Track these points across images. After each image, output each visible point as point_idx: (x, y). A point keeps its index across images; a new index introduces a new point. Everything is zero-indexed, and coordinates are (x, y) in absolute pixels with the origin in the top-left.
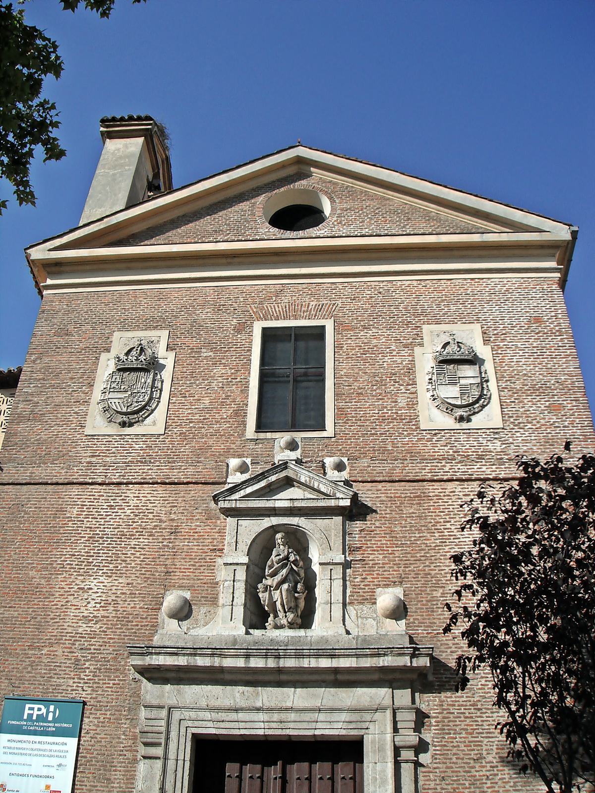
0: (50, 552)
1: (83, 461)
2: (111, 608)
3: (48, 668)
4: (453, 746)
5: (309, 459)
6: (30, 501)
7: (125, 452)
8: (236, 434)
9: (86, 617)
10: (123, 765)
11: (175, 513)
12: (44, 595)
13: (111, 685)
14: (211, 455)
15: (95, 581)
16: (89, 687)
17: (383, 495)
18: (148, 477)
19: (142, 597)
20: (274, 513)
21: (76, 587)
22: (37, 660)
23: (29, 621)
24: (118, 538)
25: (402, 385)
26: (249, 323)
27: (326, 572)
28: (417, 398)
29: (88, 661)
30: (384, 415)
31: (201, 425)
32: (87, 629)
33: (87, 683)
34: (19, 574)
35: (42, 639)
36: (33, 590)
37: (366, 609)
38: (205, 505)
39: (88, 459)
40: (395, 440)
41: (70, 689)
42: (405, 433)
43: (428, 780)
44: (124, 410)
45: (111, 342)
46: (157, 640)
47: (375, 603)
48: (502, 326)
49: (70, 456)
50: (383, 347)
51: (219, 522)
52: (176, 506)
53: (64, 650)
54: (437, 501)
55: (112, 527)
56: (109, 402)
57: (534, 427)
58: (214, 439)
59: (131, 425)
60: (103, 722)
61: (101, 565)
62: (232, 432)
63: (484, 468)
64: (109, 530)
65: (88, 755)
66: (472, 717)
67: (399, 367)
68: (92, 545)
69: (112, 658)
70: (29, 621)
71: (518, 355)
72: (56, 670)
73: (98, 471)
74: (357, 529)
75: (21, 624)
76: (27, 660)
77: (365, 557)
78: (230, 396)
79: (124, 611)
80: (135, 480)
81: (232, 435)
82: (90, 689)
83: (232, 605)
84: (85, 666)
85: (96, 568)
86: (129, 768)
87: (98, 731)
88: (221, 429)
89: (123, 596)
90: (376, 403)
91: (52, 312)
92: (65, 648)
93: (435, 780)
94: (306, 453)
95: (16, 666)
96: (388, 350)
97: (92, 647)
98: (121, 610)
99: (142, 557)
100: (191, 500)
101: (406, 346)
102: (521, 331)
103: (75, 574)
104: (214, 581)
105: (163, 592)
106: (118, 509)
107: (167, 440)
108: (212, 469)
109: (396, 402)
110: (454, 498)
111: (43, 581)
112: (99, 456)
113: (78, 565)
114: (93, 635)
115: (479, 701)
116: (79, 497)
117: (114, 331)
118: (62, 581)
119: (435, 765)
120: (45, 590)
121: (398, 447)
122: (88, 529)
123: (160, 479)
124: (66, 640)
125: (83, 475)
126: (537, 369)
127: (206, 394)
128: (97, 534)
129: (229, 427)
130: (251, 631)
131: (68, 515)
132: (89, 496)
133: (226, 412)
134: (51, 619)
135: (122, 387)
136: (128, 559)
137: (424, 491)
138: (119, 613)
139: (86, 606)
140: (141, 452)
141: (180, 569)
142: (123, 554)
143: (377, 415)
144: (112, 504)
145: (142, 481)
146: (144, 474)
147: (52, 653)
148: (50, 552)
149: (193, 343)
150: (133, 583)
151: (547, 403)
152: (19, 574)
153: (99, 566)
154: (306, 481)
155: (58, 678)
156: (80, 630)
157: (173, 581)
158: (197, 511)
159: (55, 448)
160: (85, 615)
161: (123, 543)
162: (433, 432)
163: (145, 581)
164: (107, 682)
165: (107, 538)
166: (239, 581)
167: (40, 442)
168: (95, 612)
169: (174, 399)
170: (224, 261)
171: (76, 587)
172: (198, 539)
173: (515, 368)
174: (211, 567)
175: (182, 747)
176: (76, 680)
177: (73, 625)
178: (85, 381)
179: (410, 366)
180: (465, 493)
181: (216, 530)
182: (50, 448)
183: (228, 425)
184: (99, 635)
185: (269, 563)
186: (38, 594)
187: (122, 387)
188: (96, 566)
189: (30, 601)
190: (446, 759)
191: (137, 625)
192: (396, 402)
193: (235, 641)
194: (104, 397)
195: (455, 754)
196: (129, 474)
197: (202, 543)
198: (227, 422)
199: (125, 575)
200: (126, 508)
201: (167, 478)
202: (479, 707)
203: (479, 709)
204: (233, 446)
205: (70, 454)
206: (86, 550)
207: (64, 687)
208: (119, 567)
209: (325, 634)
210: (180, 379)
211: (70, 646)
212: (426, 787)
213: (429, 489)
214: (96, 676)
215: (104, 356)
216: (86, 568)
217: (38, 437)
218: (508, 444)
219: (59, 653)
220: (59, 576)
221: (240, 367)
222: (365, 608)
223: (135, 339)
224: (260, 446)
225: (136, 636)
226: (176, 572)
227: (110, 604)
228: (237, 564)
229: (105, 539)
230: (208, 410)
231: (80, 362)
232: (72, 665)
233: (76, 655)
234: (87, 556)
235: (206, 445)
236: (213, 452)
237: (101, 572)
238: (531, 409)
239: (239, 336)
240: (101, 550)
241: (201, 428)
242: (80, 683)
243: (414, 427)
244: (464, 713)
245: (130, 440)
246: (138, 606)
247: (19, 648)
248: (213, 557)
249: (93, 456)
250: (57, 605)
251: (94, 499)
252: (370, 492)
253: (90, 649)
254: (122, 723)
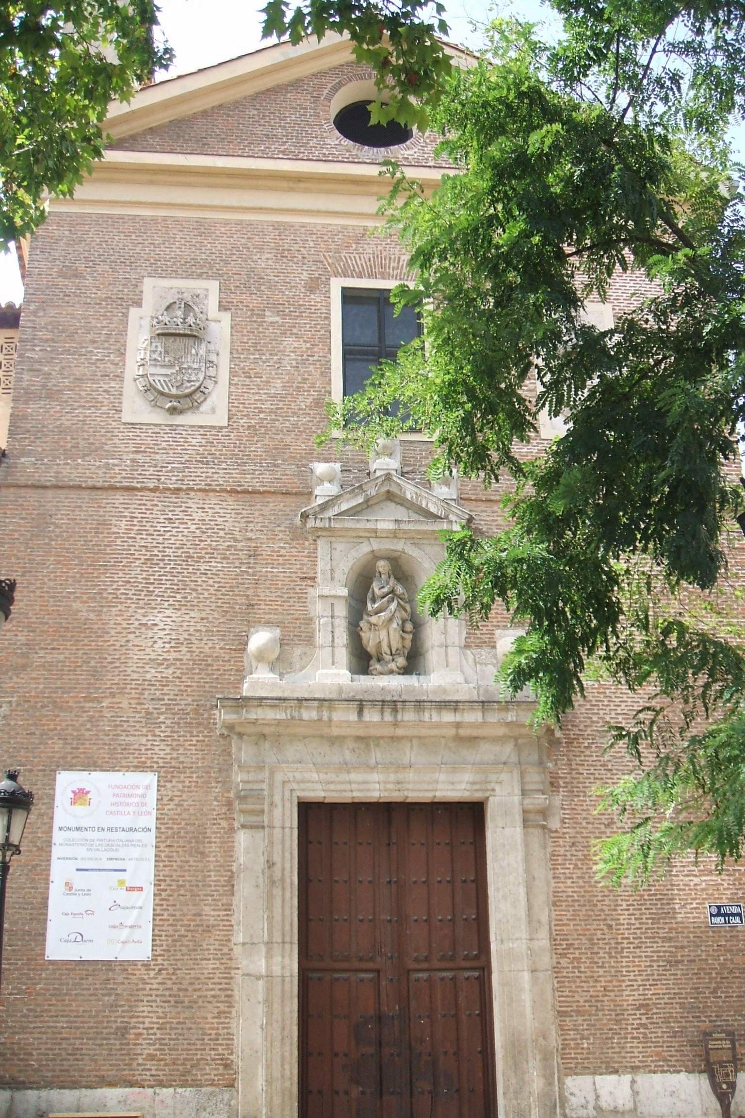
0: (97, 577)
1: (124, 457)
2: (184, 649)
3: (113, 724)
4: (583, 810)
5: (411, 468)
6: (59, 510)
7: (179, 448)
9: (154, 660)
10: (219, 835)
11: (252, 530)
12: (96, 632)
13: (194, 742)
14: (290, 457)
15: (160, 615)
16: (167, 745)
17: (499, 518)
18: (213, 483)
19: (222, 635)
20: (374, 535)
21: (137, 623)
22: (97, 715)
23: (80, 666)
24: (184, 561)
26: (323, 278)
29: (162, 713)
31: (274, 417)
32: (156, 675)
33: (164, 740)
34: (59, 606)
35: (100, 688)
36: (80, 627)
37: (484, 653)
38: (288, 522)
39: (131, 456)
41: (143, 748)
43: (557, 846)
44: (174, 391)
45: (142, 292)
46: (246, 690)
47: (494, 647)
49: (106, 451)
51: (307, 543)
52: (252, 522)
53: (131, 701)
55: (173, 546)
56: (151, 379)
59: (181, 412)
60: (189, 787)
61: (166, 595)
64: (171, 551)
65: (175, 826)
66: (602, 779)
68: (151, 570)
69: (192, 710)
70: (80, 666)
72: (122, 726)
73: (147, 473)
75: (70, 671)
76: (84, 715)
78: (306, 379)
79: (201, 652)
80: (198, 487)
82: (169, 748)
83: (333, 646)
84: (160, 720)
85: (159, 599)
86: (226, 840)
87: (184, 797)
88: (300, 423)
89: (198, 634)
91: (48, 240)
92: (133, 698)
93: (565, 846)
95: (70, 723)
97: (166, 697)
98: (198, 650)
99: (216, 585)
100: (270, 515)
103: (133, 606)
104: (308, 616)
105: (246, 629)
106: (180, 523)
107: (232, 435)
108: (294, 475)
111: (92, 616)
112: (146, 452)
113: (135, 594)
114: (165, 682)
115: (610, 761)
116: (126, 506)
117: (143, 277)
118: (116, 615)
119: (565, 830)
120: (96, 626)
122: (144, 549)
123: (229, 486)
124: (131, 689)
125: (128, 478)
127: (276, 374)
128: (156, 555)
129: (310, 421)
130: (356, 677)
131: (115, 530)
132: (140, 505)
133: (305, 401)
134: (109, 663)
135: (167, 359)
136: (199, 588)
138: (194, 654)
139: (152, 646)
140: (201, 449)
141: (265, 600)
142: (192, 581)
144: (170, 516)
145: (207, 488)
146: (208, 480)
147: (116, 706)
148: (97, 577)
149: (254, 302)
150: (207, 618)
152: (59, 606)
153: (163, 596)
154: (412, 497)
155: (127, 736)
156: (148, 676)
157: (258, 616)
158: (279, 528)
159: (84, 439)
160: (153, 657)
161: (191, 568)
163: (223, 616)
164: (189, 738)
165: (169, 560)
166: (338, 617)
167: (62, 431)
168: (165, 654)
169: (236, 379)
170: (285, 184)
171: (137, 623)
172: (284, 564)
174: (302, 597)
175: (288, 813)
176: (150, 738)
177: (138, 670)
178: (112, 347)
181: (305, 554)
182: (77, 439)
183: (308, 419)
184: (172, 682)
185: (370, 595)
186: (88, 631)
187: (167, 359)
188: (159, 596)
189: (78, 641)
190: (576, 823)
191: (219, 670)
193: (340, 689)
194: (143, 371)
195: (585, 819)
196: (189, 478)
197: (289, 568)
198: (306, 414)
199: (196, 608)
200: (190, 523)
201: (239, 486)
202: (610, 767)
203: (610, 770)
205: (106, 447)
206: (144, 576)
207: (136, 747)
208: (189, 598)
210: (240, 351)
211: (137, 696)
212: (556, 853)
214: (174, 732)
215: (134, 312)
216: (146, 598)
217: (58, 423)
219: (125, 704)
220: (113, 609)
221: (317, 340)
222: (483, 653)
223: (174, 291)
225: (218, 683)
226: (260, 605)
227: (182, 644)
228: (335, 597)
229: (166, 562)
230: (283, 398)
231: (102, 318)
232: (142, 720)
233: (146, 707)
234: (146, 583)
237: (166, 603)
239: (312, 296)
240: (163, 575)
241: (274, 420)
242: (155, 741)
244: (594, 774)
245: (184, 433)
246: (218, 647)
247: (71, 700)
248: (303, 587)
249: (137, 452)
250: (114, 645)
251: (147, 509)
252: (485, 514)
253: (164, 700)
254: (212, 787)
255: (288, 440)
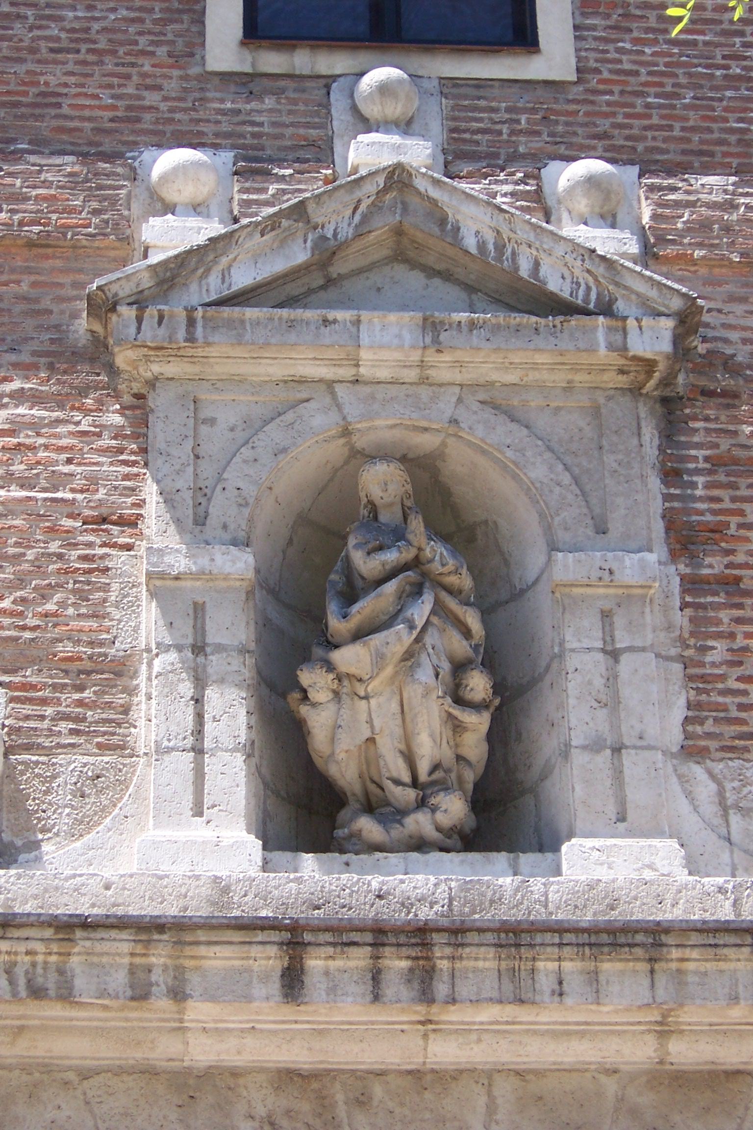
8: (162, 51)
27: (586, 623)
58: (70, 67)
62: (143, 41)
74: (701, 453)
77: (740, 566)
81: (143, 53)
88: (96, 26)
94: (465, 141)
129: (133, 20)
158: (13, 357)
166: (220, 648)
204: (151, 98)
209: (603, 874)
224: (269, 102)
235: (33, 90)
236: (65, 117)
255: (53, 78)
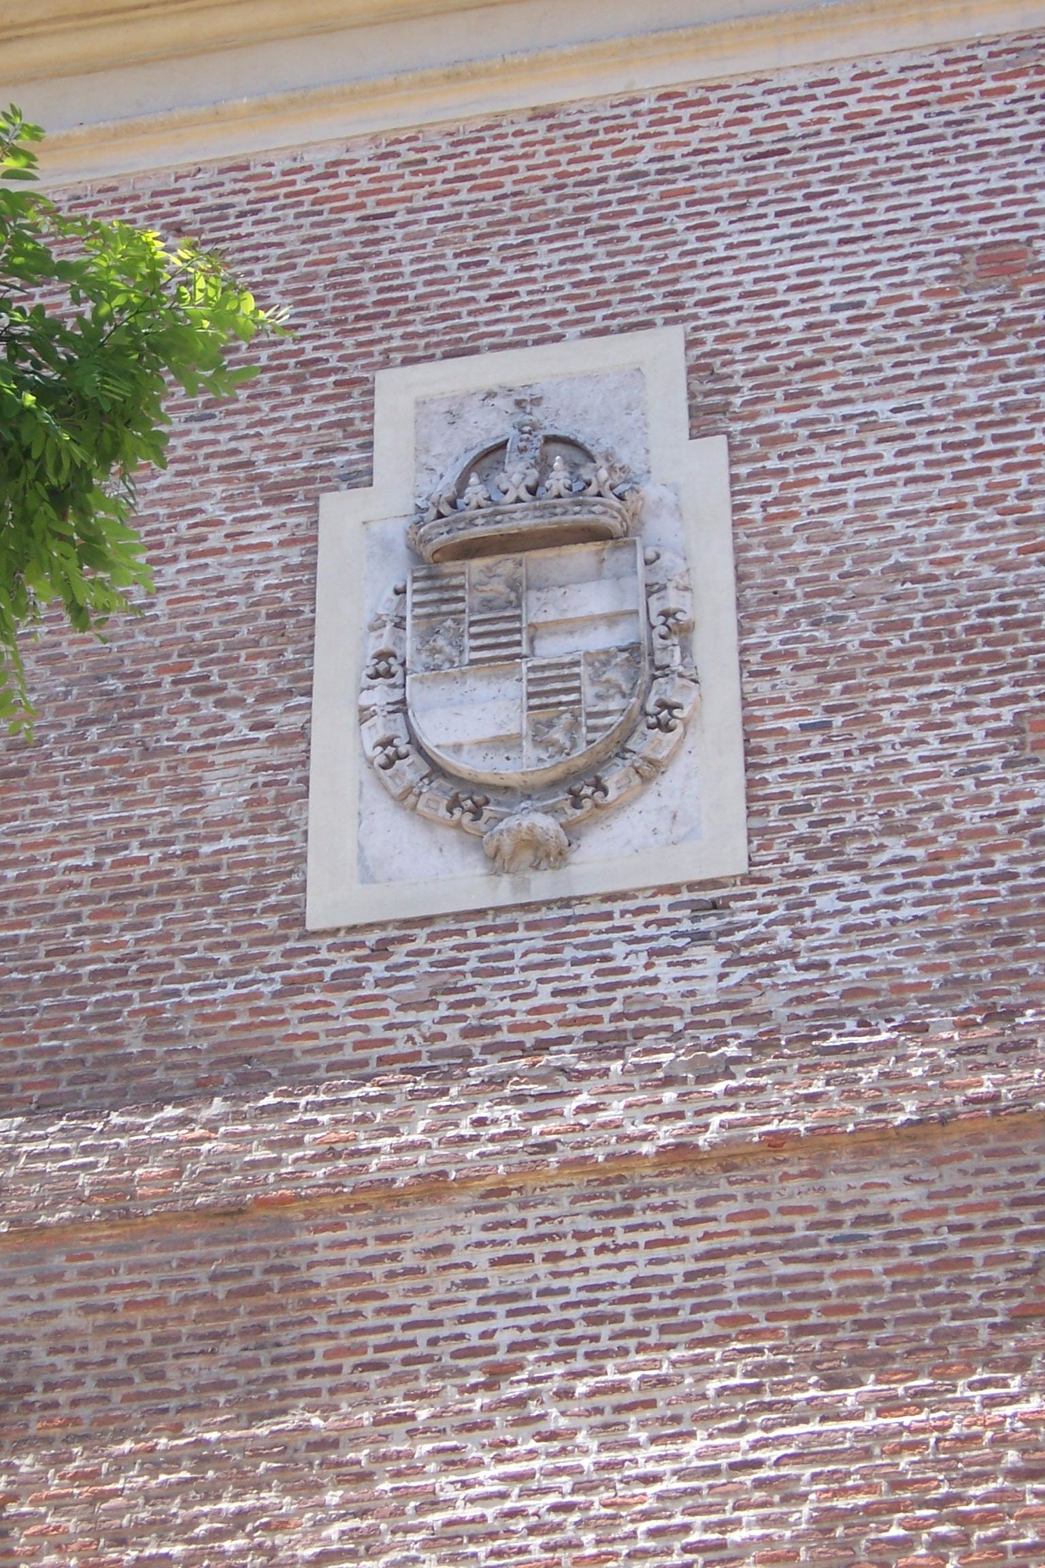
25: (237, 702)
28: (305, 763)
30: (122, 871)
40: (168, 1002)
42: (225, 957)
48: (797, 323)
50: (162, 511)
54: (352, 1307)
57: (919, 852)
63: (616, 1109)
67: (228, 607)
71: (870, 467)
90: (92, 816)
96: (183, 524)
101: (277, 495)
102: (900, 337)
109: (196, 795)
110: (441, 1286)
121: (179, 1037)
126: (969, 533)
137: (288, 1259)
143: (87, 878)
151: (1007, 714)
162: (371, 938)
173: (846, 541)
179: (287, 595)
180: (501, 1252)
192: (196, 795)
213: (312, 1247)
218: (764, 957)
238: (912, 755)
243: (272, 921)
